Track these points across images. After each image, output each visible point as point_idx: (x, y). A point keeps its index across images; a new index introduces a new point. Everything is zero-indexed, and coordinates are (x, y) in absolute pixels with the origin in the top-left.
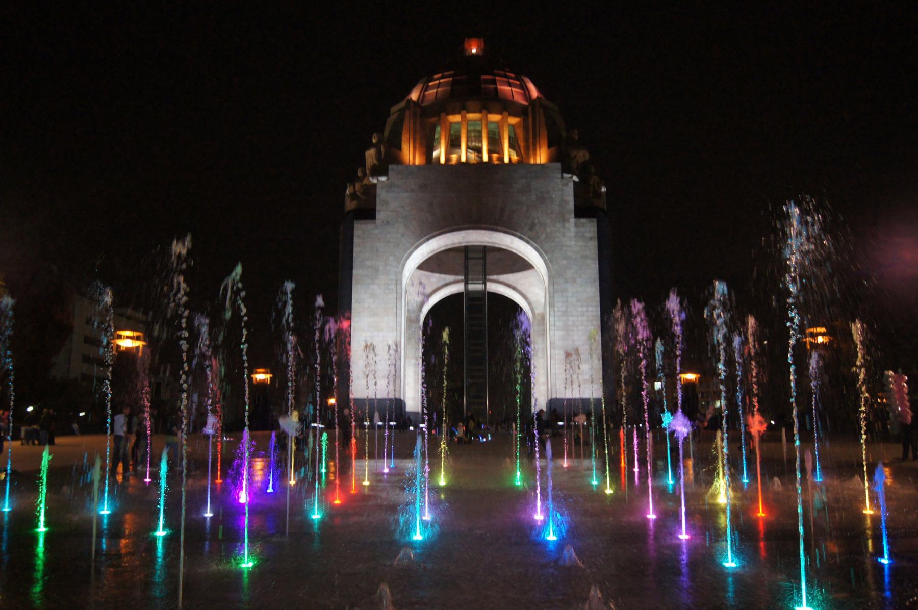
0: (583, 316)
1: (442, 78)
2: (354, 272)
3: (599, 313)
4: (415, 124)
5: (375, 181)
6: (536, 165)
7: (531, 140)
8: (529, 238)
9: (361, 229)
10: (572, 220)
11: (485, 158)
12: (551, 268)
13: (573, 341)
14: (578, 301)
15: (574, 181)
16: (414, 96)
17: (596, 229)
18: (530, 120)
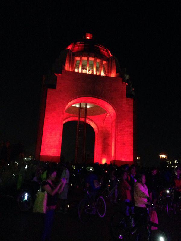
0: (127, 131)
1: (80, 44)
2: (47, 107)
3: (133, 131)
4: (70, 57)
5: (57, 75)
6: (111, 77)
7: (110, 70)
8: (110, 102)
9: (50, 91)
10: (125, 98)
11: (95, 73)
12: (118, 114)
13: (124, 140)
14: (126, 126)
15: (127, 85)
16: (70, 48)
17: (133, 102)
18: (110, 63)
